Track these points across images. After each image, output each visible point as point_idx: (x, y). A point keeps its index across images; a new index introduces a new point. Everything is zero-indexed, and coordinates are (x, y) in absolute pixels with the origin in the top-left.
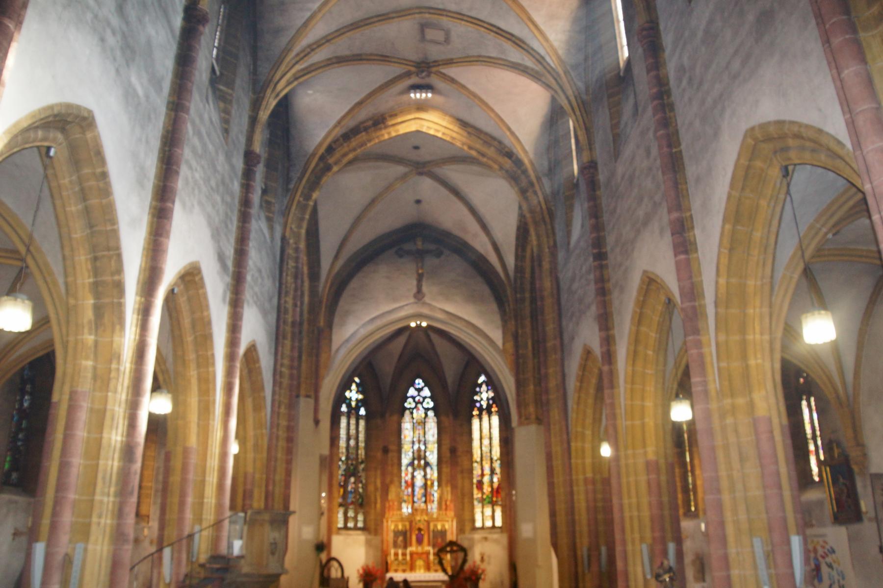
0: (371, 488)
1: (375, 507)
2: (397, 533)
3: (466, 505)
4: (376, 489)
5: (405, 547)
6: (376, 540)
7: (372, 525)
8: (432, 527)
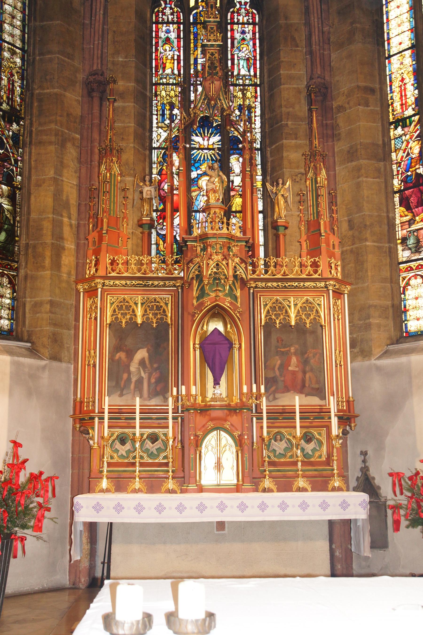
0: (41, 200)
1: (57, 265)
2: (125, 335)
3: (371, 259)
4: (60, 205)
5: (161, 389)
6: (54, 376)
7: (40, 322)
8: (262, 317)
